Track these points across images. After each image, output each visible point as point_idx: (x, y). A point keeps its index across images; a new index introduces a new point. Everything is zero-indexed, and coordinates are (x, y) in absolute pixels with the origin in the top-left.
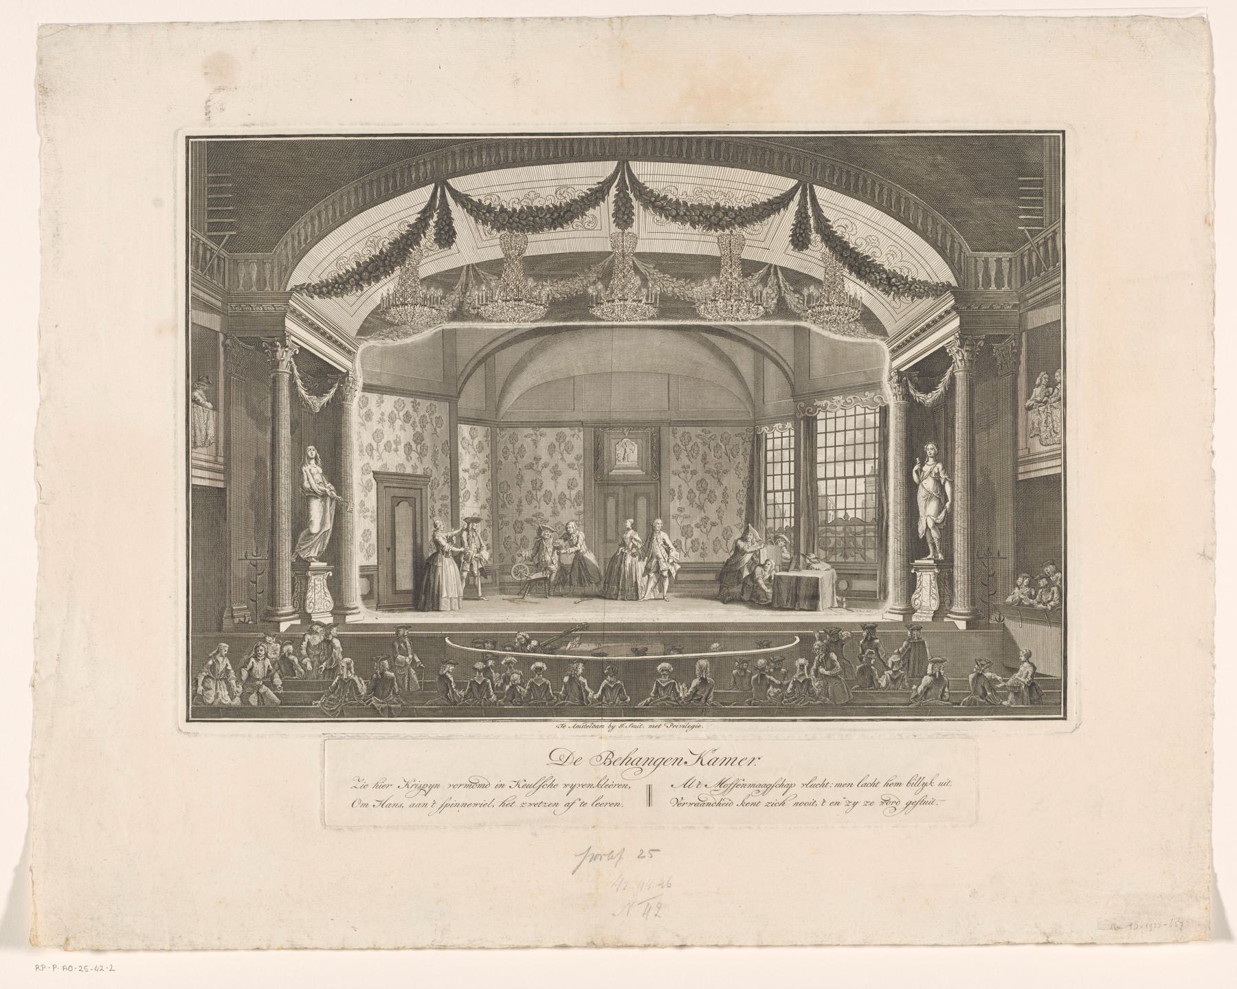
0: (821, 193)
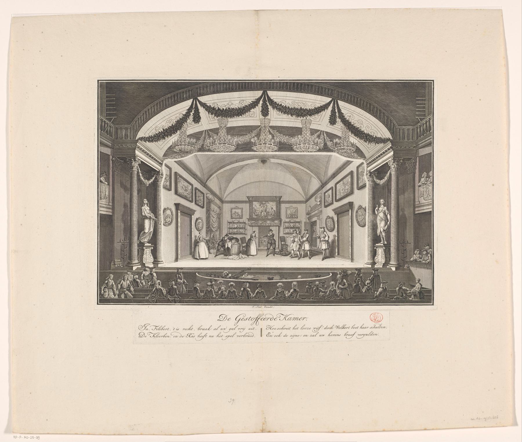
0: (340, 103)
